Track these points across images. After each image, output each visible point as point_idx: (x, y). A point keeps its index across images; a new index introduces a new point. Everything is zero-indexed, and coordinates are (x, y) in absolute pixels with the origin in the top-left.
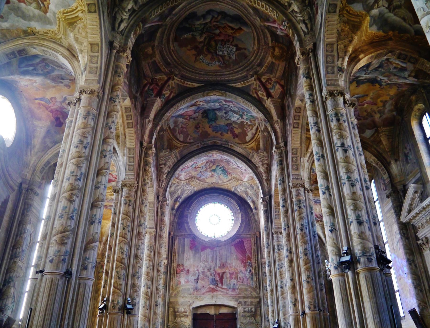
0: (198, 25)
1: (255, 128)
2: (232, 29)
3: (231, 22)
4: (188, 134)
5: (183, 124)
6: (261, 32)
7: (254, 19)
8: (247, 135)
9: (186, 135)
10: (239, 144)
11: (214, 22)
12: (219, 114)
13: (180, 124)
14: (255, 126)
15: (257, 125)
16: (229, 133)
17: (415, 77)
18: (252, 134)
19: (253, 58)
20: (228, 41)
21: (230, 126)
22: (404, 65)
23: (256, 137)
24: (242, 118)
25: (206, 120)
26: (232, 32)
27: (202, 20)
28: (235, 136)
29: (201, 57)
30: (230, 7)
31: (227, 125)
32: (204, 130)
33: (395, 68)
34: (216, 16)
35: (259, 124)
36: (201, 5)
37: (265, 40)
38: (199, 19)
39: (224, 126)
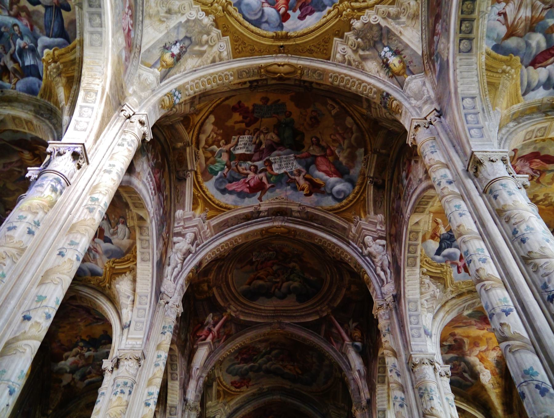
0: (296, 281)
1: (203, 144)
2: (259, 278)
5: (340, 145)
6: (228, 297)
7: (238, 311)
8: (213, 124)
10: (227, 99)
11: (278, 282)
12: (273, 136)
13: (345, 147)
14: (204, 148)
15: (201, 151)
17: (69, 384)
19: (231, 266)
24: (229, 152)
26: (259, 275)
27: (291, 286)
28: (239, 108)
29: (296, 252)
30: (263, 308)
31: (256, 120)
33: (90, 373)
34: (277, 290)
35: (197, 157)
36: (292, 308)
37: (221, 290)
39: (262, 117)
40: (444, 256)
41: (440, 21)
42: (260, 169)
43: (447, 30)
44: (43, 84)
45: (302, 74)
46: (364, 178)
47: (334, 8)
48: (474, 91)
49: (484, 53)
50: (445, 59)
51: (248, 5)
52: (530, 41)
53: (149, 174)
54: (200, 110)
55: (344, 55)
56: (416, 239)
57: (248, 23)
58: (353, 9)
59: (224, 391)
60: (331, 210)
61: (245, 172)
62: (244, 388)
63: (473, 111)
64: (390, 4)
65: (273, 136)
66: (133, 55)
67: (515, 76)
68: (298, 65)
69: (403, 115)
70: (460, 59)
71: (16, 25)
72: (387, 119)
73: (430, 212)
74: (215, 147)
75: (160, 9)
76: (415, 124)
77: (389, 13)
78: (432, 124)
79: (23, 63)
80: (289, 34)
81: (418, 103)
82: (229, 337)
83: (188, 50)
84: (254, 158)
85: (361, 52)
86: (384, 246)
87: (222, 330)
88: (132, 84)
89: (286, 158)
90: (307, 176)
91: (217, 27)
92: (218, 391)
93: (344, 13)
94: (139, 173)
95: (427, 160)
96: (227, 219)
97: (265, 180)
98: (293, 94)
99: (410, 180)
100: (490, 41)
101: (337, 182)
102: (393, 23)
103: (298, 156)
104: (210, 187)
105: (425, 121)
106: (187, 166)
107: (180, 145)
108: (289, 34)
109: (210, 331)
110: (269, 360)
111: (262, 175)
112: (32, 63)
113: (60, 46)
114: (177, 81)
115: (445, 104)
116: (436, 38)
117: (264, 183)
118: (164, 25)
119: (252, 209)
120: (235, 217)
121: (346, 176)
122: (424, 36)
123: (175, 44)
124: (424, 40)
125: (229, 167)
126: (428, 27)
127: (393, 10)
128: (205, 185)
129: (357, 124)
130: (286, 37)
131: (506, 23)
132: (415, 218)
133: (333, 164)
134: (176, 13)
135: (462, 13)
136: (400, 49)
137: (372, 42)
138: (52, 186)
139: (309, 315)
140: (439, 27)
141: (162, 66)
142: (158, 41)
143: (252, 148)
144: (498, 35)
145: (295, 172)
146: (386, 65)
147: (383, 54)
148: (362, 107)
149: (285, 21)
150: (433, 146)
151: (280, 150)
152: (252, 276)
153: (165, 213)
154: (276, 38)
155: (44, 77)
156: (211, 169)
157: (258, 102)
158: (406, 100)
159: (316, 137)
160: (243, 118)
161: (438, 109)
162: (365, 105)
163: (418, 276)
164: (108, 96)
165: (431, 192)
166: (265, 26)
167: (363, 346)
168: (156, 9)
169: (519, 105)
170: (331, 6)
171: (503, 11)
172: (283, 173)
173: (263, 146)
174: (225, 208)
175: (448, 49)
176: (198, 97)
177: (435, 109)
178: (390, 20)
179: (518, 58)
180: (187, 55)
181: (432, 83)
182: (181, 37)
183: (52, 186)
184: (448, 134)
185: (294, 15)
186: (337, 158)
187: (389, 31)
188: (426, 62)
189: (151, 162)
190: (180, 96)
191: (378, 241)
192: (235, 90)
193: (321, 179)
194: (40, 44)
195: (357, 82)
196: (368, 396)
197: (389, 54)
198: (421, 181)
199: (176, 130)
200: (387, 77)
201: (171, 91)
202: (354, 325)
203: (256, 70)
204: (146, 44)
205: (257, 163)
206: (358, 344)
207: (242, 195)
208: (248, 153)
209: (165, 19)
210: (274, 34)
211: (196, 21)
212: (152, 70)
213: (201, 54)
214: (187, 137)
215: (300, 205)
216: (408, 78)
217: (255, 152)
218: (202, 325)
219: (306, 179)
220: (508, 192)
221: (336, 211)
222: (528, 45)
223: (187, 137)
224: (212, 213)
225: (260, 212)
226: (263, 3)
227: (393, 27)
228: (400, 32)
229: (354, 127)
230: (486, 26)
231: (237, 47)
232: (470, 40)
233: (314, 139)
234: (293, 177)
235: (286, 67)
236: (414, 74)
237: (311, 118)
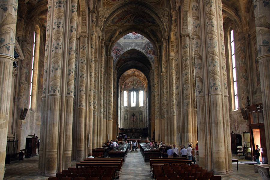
59: (107, 3)
92: (104, 3)
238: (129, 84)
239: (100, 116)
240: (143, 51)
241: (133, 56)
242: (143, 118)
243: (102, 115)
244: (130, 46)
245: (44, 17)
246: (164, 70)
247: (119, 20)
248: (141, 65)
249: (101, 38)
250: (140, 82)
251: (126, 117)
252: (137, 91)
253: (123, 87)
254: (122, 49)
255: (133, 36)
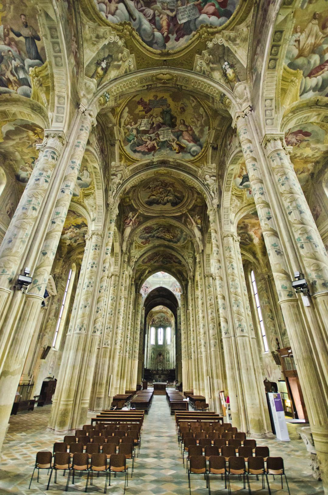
1: (122, 124)
2: (153, 195)
3: (154, 199)
4: (193, 107)
5: (196, 125)
8: (128, 112)
9: (196, 108)
10: (134, 97)
11: (162, 197)
12: (160, 119)
13: (198, 125)
14: (123, 127)
15: (122, 129)
16: (148, 102)
17: (69, 244)
18: (123, 117)
20: (154, 188)
21: (148, 110)
22: (77, 243)
23: (119, 116)
25: (172, 113)
28: (141, 102)
31: (150, 109)
32: (176, 103)
33: (78, 239)
38: (170, 200)
39: (154, 108)
40: (244, 186)
41: (260, 45)
42: (153, 138)
43: (263, 52)
44: (32, 90)
45: (176, 80)
46: (207, 144)
47: (197, 32)
48: (273, 95)
49: (282, 69)
50: (259, 73)
51: (145, 30)
52: (311, 60)
53: (97, 144)
54: (120, 104)
55: (201, 67)
56: (231, 178)
57: (145, 44)
58: (209, 33)
59: (138, 246)
60: (189, 161)
61: (145, 140)
62: (147, 244)
63: (269, 108)
64: (231, 30)
65: (160, 119)
66: (80, 70)
67: (297, 84)
68: (174, 73)
69: (231, 109)
70: (268, 74)
71: (9, 51)
72: (223, 109)
73: (239, 163)
74: (129, 126)
75: (92, 35)
76: (237, 115)
77: (230, 37)
78: (246, 115)
79: (19, 76)
80: (169, 52)
81: (241, 101)
82: (140, 223)
83: (111, 65)
84: (150, 132)
85: (211, 65)
86: (215, 180)
87: (136, 220)
88: (82, 90)
89: (167, 132)
90: (178, 142)
91: (127, 48)
92: (136, 246)
93: (203, 36)
94: (92, 144)
95: (241, 138)
96: (137, 166)
97: (156, 145)
98: (171, 93)
99: (231, 146)
100: (287, 60)
101: (193, 146)
102: (232, 44)
103: (173, 131)
104: (127, 149)
105: (243, 113)
106: (115, 138)
107: (110, 125)
108: (169, 52)
109: (131, 220)
110: (158, 232)
111: (154, 142)
112: (24, 77)
113: (38, 65)
114: (107, 87)
115: (255, 103)
116: (256, 57)
117: (155, 147)
118: (96, 47)
119: (149, 161)
120: (141, 165)
121: (198, 143)
122: (249, 55)
123: (103, 61)
124: (249, 57)
125: (137, 137)
126: (253, 48)
127: (232, 34)
128: (125, 148)
129: (206, 112)
130: (168, 54)
131: (298, 48)
132: (232, 167)
133: (191, 135)
134: (102, 38)
135: (274, 41)
136: (234, 64)
137: (218, 58)
138: (52, 156)
139: (177, 212)
140: (259, 49)
141: (97, 76)
142: (94, 59)
143: (149, 126)
144: (293, 55)
145: (171, 140)
146: (225, 75)
147: (224, 66)
148: (209, 102)
149: (167, 42)
150: (245, 129)
151: (164, 127)
152: (150, 194)
153: (106, 164)
154: (162, 55)
155: (32, 86)
156: (128, 139)
157: (152, 99)
158: (234, 98)
159: (183, 120)
160: (144, 108)
161: (251, 106)
162: (211, 100)
163: (230, 196)
164: (71, 100)
165: (240, 154)
166: (155, 45)
167: (202, 227)
168: (90, 35)
169: (297, 102)
170: (195, 31)
171: (298, 39)
172: (165, 141)
173: (155, 125)
174: (136, 160)
175: (262, 66)
176: (118, 96)
177: (250, 106)
178: (230, 42)
179: (302, 72)
180: (110, 68)
181: (250, 88)
182: (106, 56)
183: (52, 156)
184: (254, 122)
185: (173, 37)
186: (194, 132)
187: (229, 50)
188: (248, 73)
189: (97, 136)
190: (109, 96)
191: (212, 178)
192: (139, 91)
193: (185, 144)
194: (26, 65)
195: (207, 86)
196: (203, 248)
197: (228, 66)
198: (237, 147)
199: (108, 116)
200: (224, 83)
201: (104, 93)
202: (198, 217)
203: (150, 78)
204: (86, 61)
205: (151, 135)
206: (199, 226)
207: (144, 153)
208: (147, 129)
209: (96, 43)
210: (161, 52)
211: (115, 43)
212: (92, 79)
213: (118, 67)
214: (114, 120)
215: (174, 159)
216: (237, 84)
217: (150, 129)
218: (127, 218)
219: (177, 144)
220: (280, 158)
221: (192, 162)
222: (309, 62)
223: (114, 120)
224: (129, 163)
225: (153, 162)
226: (154, 28)
227: (232, 47)
228: (236, 52)
229: (204, 114)
230: (286, 50)
231: (139, 61)
232: (276, 60)
233: (182, 121)
234: (170, 143)
235: (167, 75)
236: (240, 81)
237: (181, 108)
238: (157, 320)
239: (125, 356)
240: (171, 289)
241: (161, 293)
242: (170, 357)
243: (127, 354)
244: (158, 284)
245: (80, 256)
246: (190, 308)
247: (149, 260)
248: (168, 302)
249: (131, 276)
250: (167, 319)
251: (153, 356)
252: (165, 327)
253: (151, 323)
254: (151, 286)
255: (161, 274)
